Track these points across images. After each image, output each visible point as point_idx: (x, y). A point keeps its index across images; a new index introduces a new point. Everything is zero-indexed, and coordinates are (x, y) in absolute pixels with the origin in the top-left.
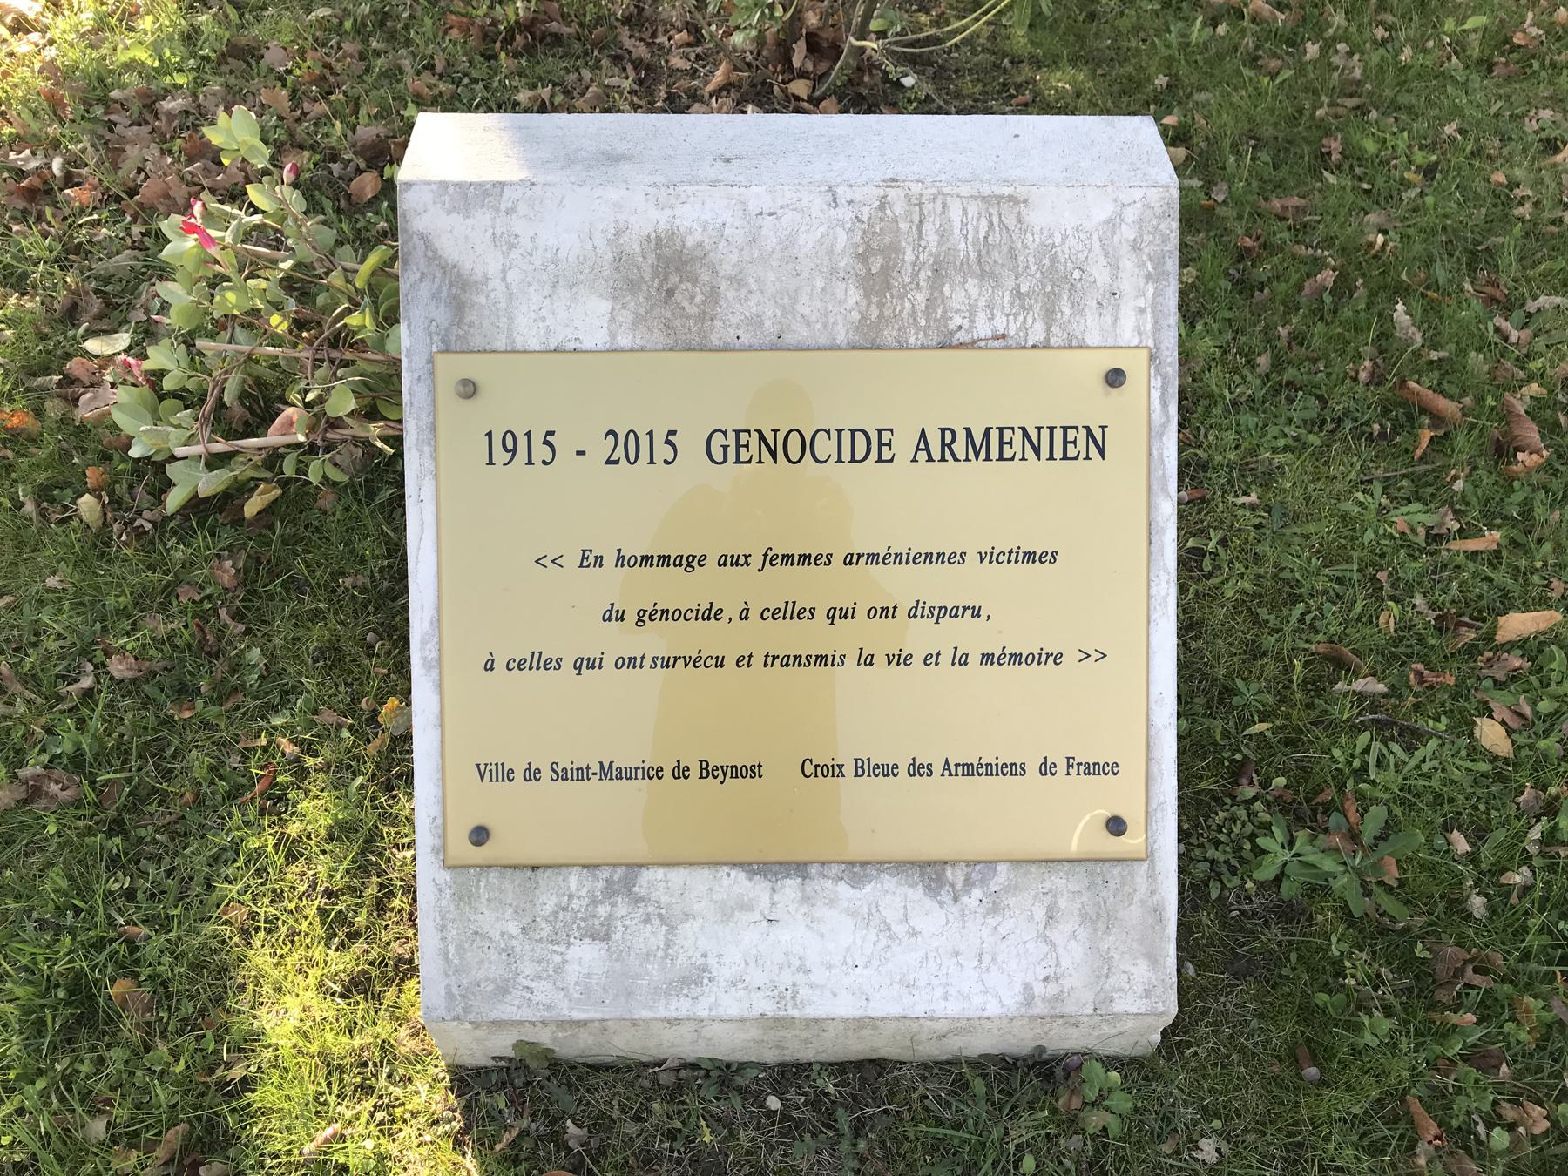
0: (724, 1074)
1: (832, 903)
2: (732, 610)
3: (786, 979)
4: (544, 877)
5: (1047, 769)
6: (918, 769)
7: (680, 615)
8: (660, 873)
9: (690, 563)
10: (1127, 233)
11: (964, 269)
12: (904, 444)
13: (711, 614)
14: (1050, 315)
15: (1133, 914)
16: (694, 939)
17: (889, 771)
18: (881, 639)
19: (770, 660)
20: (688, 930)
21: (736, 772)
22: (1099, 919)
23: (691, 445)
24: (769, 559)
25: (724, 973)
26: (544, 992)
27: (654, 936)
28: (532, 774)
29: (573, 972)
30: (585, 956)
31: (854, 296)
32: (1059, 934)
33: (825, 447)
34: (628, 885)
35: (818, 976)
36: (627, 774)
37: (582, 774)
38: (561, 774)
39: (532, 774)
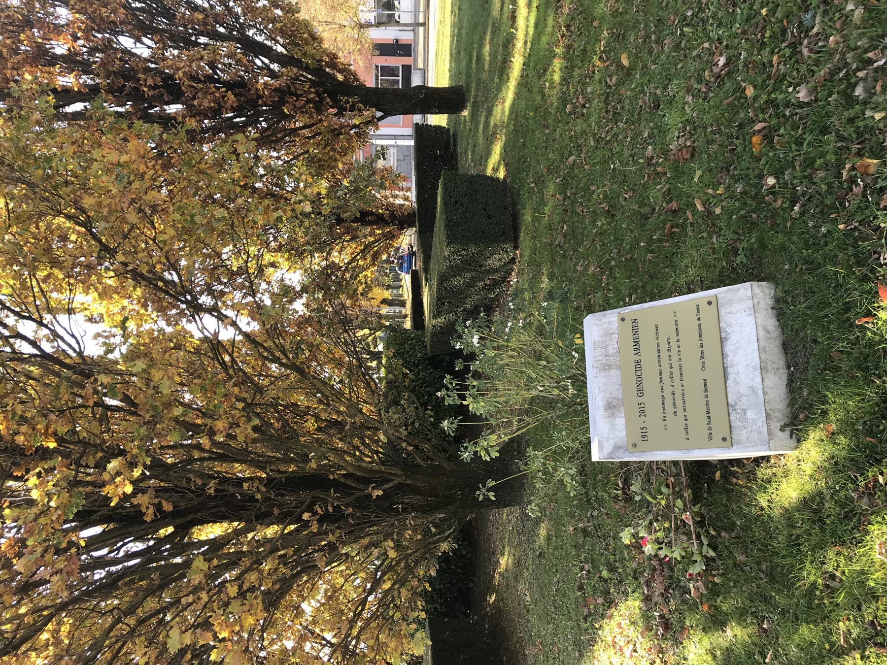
0: (790, 381)
1: (732, 360)
2: (672, 389)
3: (751, 369)
4: (732, 425)
5: (699, 319)
6: (702, 346)
7: (674, 399)
8: (729, 399)
9: (663, 398)
10: (598, 322)
11: (606, 351)
12: (637, 358)
13: (673, 393)
14: (613, 334)
15: (729, 296)
16: (744, 390)
17: (702, 352)
18: (675, 357)
19: (682, 380)
20: (741, 392)
21: (705, 385)
22: (730, 302)
23: (640, 400)
24: (661, 382)
25: (751, 383)
26: (759, 423)
27: (744, 399)
28: (710, 429)
29: (754, 417)
30: (750, 414)
31: (612, 371)
32: (734, 310)
33: (639, 373)
34: (732, 406)
35: (749, 362)
36: (708, 408)
37: (709, 418)
38: (709, 423)
39: (710, 429)
